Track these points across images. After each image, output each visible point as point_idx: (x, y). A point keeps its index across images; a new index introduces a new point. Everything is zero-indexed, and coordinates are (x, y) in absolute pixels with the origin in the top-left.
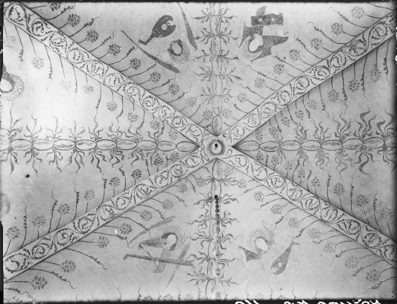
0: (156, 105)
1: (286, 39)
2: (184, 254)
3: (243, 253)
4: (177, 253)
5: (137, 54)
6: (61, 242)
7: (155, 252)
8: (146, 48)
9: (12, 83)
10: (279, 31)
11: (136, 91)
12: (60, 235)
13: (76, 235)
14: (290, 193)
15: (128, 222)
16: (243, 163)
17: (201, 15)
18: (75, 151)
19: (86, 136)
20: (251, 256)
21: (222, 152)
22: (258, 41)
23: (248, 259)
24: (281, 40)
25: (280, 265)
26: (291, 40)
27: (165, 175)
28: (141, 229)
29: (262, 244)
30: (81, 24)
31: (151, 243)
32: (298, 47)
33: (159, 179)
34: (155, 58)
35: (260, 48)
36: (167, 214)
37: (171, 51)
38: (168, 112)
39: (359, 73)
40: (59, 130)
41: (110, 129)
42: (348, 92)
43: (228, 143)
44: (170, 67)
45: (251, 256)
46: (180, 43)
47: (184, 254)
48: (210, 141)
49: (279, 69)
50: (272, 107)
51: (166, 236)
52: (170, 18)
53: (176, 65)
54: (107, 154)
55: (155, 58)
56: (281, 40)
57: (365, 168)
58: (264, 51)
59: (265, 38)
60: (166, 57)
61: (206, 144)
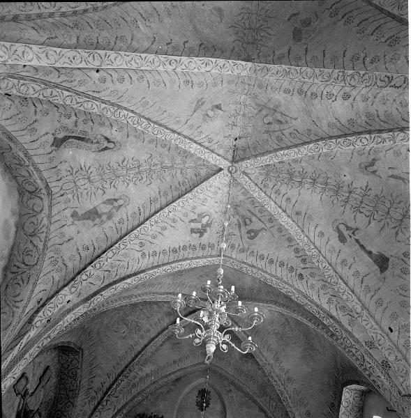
0: (263, 200)
1: (190, 222)
2: (260, 111)
3: (223, 109)
4: (264, 112)
5: (269, 225)
6: (332, 143)
7: (279, 117)
8: (263, 226)
9: (338, 228)
10: (193, 225)
11: (272, 209)
12: (332, 147)
13: (323, 145)
14: (192, 146)
15: (291, 139)
16: (218, 161)
17: (233, 236)
18: (315, 180)
19: (307, 186)
20: (218, 107)
21: (229, 167)
22: (205, 221)
23: (220, 105)
24: (192, 221)
25: (200, 103)
26: (187, 221)
27: (264, 162)
28: (284, 132)
29: (211, 113)
30: (293, 248)
31: (280, 122)
32: (183, 218)
33: (268, 160)
34: (260, 220)
35: (204, 217)
36: (266, 136)
37: (250, 220)
38: (257, 195)
39: (153, 207)
40: (321, 194)
41: (292, 187)
42: (158, 196)
43: (225, 171)
44: (252, 214)
45: (218, 107)
46: (246, 225)
47: (260, 111)
48: (236, 174)
49: (194, 208)
50: (199, 191)
51: (269, 123)
52: (249, 238)
53: (249, 214)
54: (297, 174)
55: (260, 220)
56: (192, 221)
57: (149, 156)
58: (201, 216)
59: (200, 222)
60: (254, 219)
61: (238, 173)
